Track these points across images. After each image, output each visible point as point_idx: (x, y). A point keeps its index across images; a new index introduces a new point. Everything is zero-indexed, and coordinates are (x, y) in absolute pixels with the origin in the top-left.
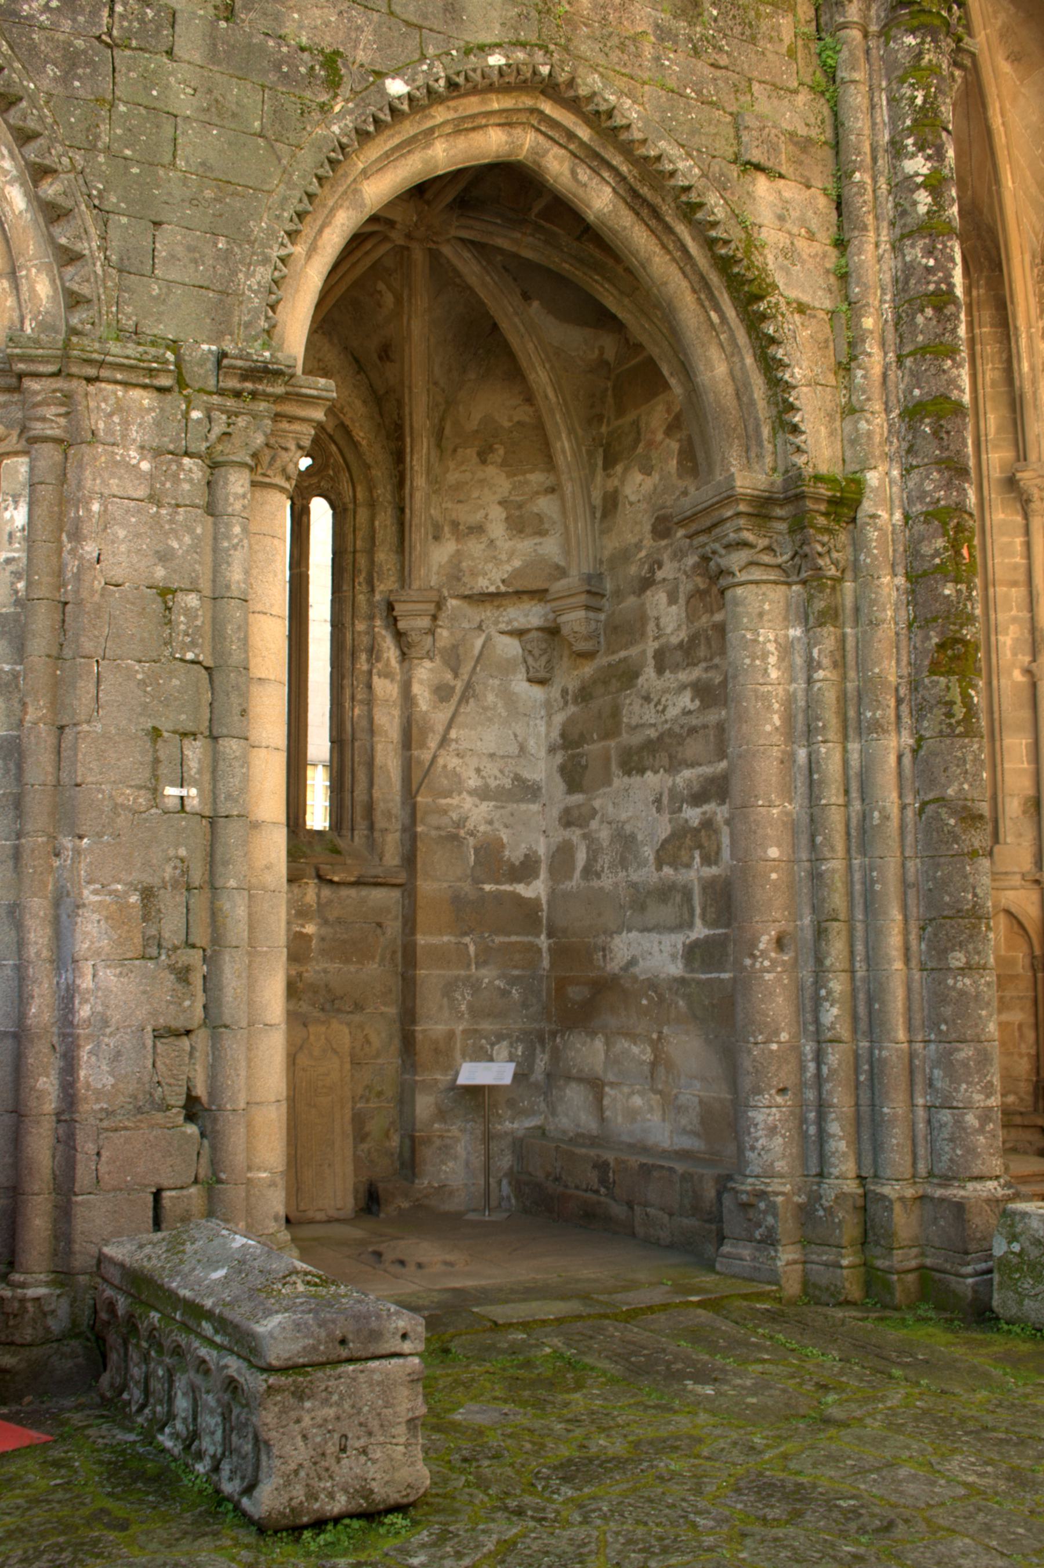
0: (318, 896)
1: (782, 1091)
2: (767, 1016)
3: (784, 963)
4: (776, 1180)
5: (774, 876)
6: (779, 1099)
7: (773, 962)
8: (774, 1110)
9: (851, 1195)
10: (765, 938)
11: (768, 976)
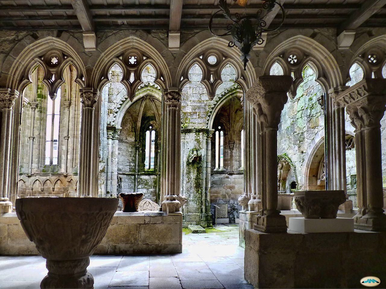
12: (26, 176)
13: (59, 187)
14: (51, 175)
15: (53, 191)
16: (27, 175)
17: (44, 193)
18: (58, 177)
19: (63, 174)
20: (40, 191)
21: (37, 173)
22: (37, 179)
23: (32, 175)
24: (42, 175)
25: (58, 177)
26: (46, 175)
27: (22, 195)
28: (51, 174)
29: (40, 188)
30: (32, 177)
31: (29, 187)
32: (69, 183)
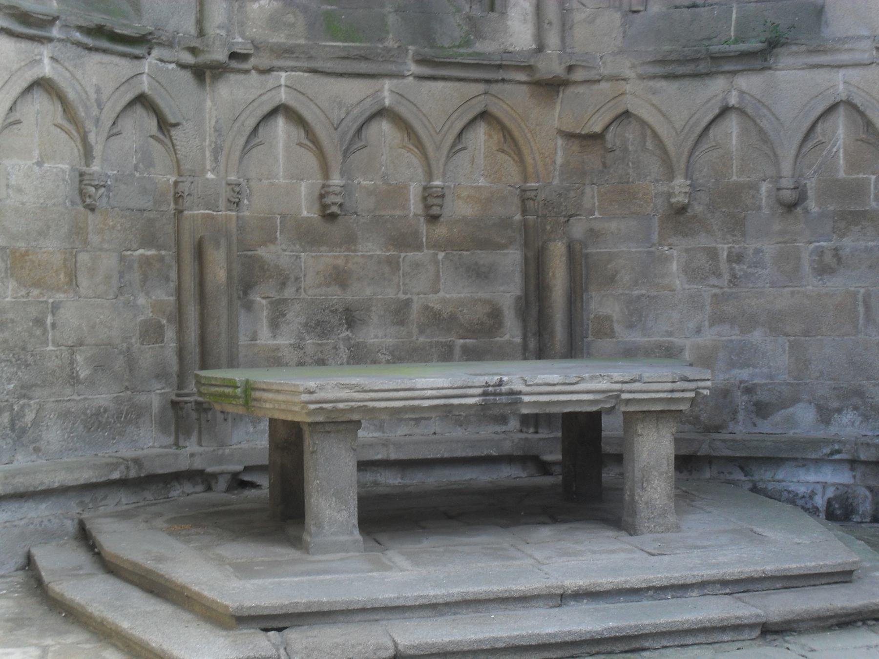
12: (183, 66)
13: (482, 182)
14: (414, 68)
15: (433, 219)
16: (188, 58)
17: (350, 240)
18: (481, 87)
19: (529, 68)
20: (305, 213)
21: (279, 38)
22: (283, 96)
23: (233, 56)
24: (329, 66)
26: (363, 67)
27: (151, 252)
28: (421, 61)
29: (304, 188)
30: (233, 78)
31: (210, 175)
32: (575, 146)
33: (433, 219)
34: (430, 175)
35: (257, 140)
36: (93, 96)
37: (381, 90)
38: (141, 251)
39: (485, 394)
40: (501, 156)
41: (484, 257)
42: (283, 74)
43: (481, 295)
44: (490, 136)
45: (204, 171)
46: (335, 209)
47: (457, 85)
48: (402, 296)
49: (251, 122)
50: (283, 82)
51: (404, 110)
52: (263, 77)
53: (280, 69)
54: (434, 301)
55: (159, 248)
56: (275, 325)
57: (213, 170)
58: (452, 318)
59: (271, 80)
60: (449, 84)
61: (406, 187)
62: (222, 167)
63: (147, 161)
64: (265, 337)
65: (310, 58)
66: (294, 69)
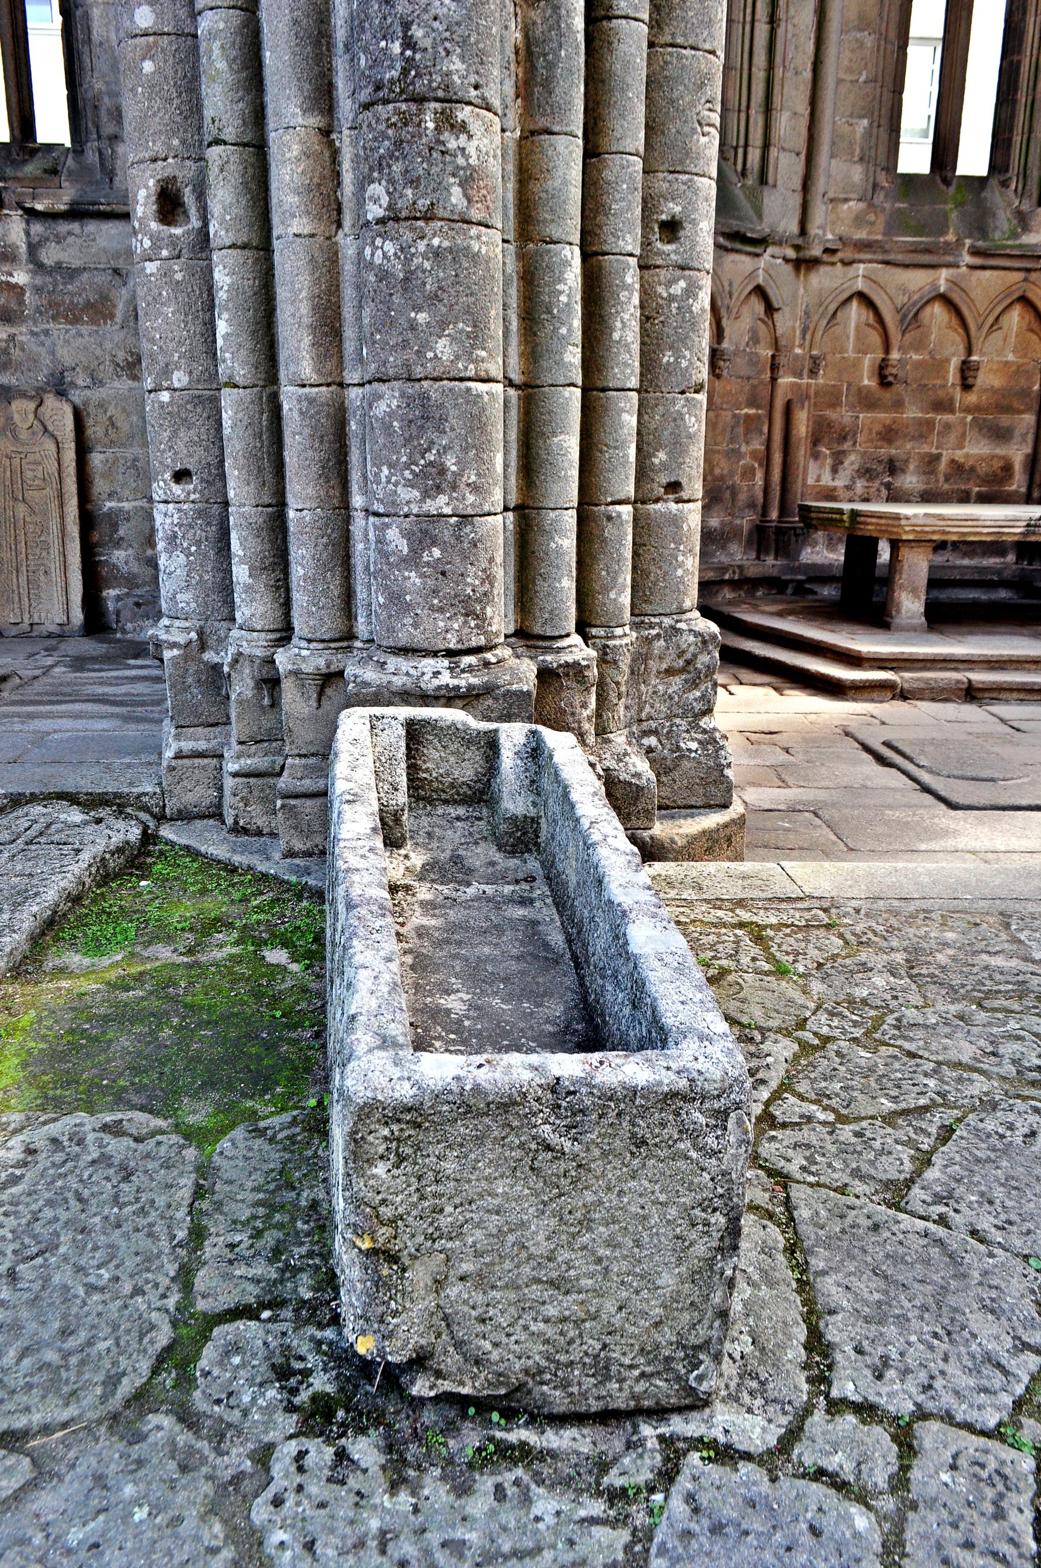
0: (27, 233)
1: (181, 476)
2: (153, 341)
3: (173, 241)
4: (177, 623)
5: (148, 66)
6: (177, 490)
7: (155, 239)
8: (171, 506)
9: (251, 658)
10: (142, 194)
11: (151, 267)
13: (1011, 357)
14: (967, 259)
16: (791, 254)
17: (898, 405)
20: (866, 382)
21: (861, 235)
22: (860, 285)
23: (826, 251)
24: (900, 258)
25: (1019, 276)
26: (926, 259)
27: (752, 411)
28: (975, 252)
31: (798, 351)
33: (967, 387)
34: (969, 351)
35: (834, 322)
36: (727, 288)
37: (938, 279)
38: (746, 411)
39: (1028, 525)
40: (1029, 335)
41: (1005, 420)
42: (862, 266)
43: (999, 451)
44: (1023, 318)
45: (793, 347)
46: (891, 379)
47: (1002, 273)
48: (934, 451)
49: (832, 308)
50: (861, 272)
51: (956, 297)
52: (846, 268)
53: (860, 261)
54: (959, 455)
55: (758, 407)
56: (835, 470)
57: (801, 346)
58: (972, 469)
59: (851, 271)
60: (996, 273)
61: (948, 361)
62: (807, 343)
63: (755, 339)
64: (827, 480)
65: (885, 252)
66: (870, 261)
